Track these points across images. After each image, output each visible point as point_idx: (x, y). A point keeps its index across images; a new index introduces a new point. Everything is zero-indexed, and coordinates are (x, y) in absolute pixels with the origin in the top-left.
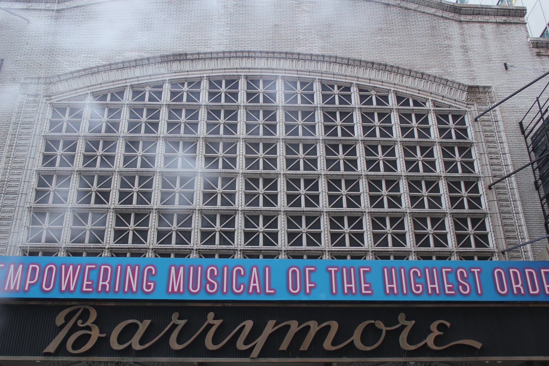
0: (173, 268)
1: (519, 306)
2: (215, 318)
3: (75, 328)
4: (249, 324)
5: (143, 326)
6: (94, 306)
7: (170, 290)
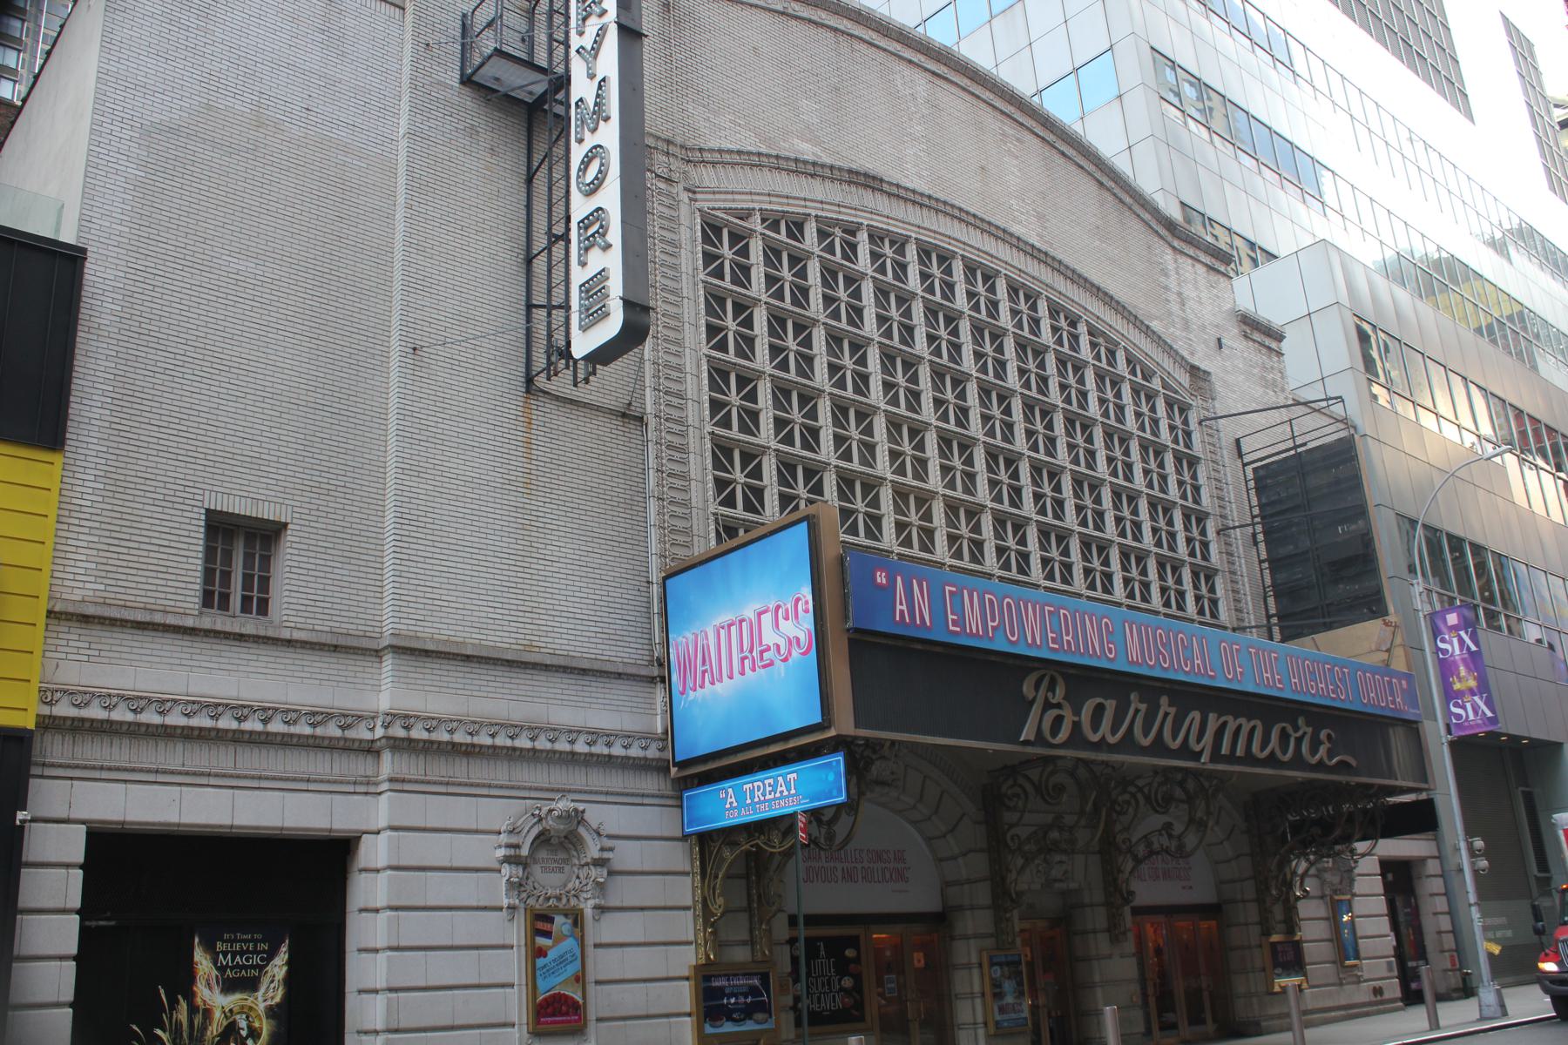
6: (1063, 675)
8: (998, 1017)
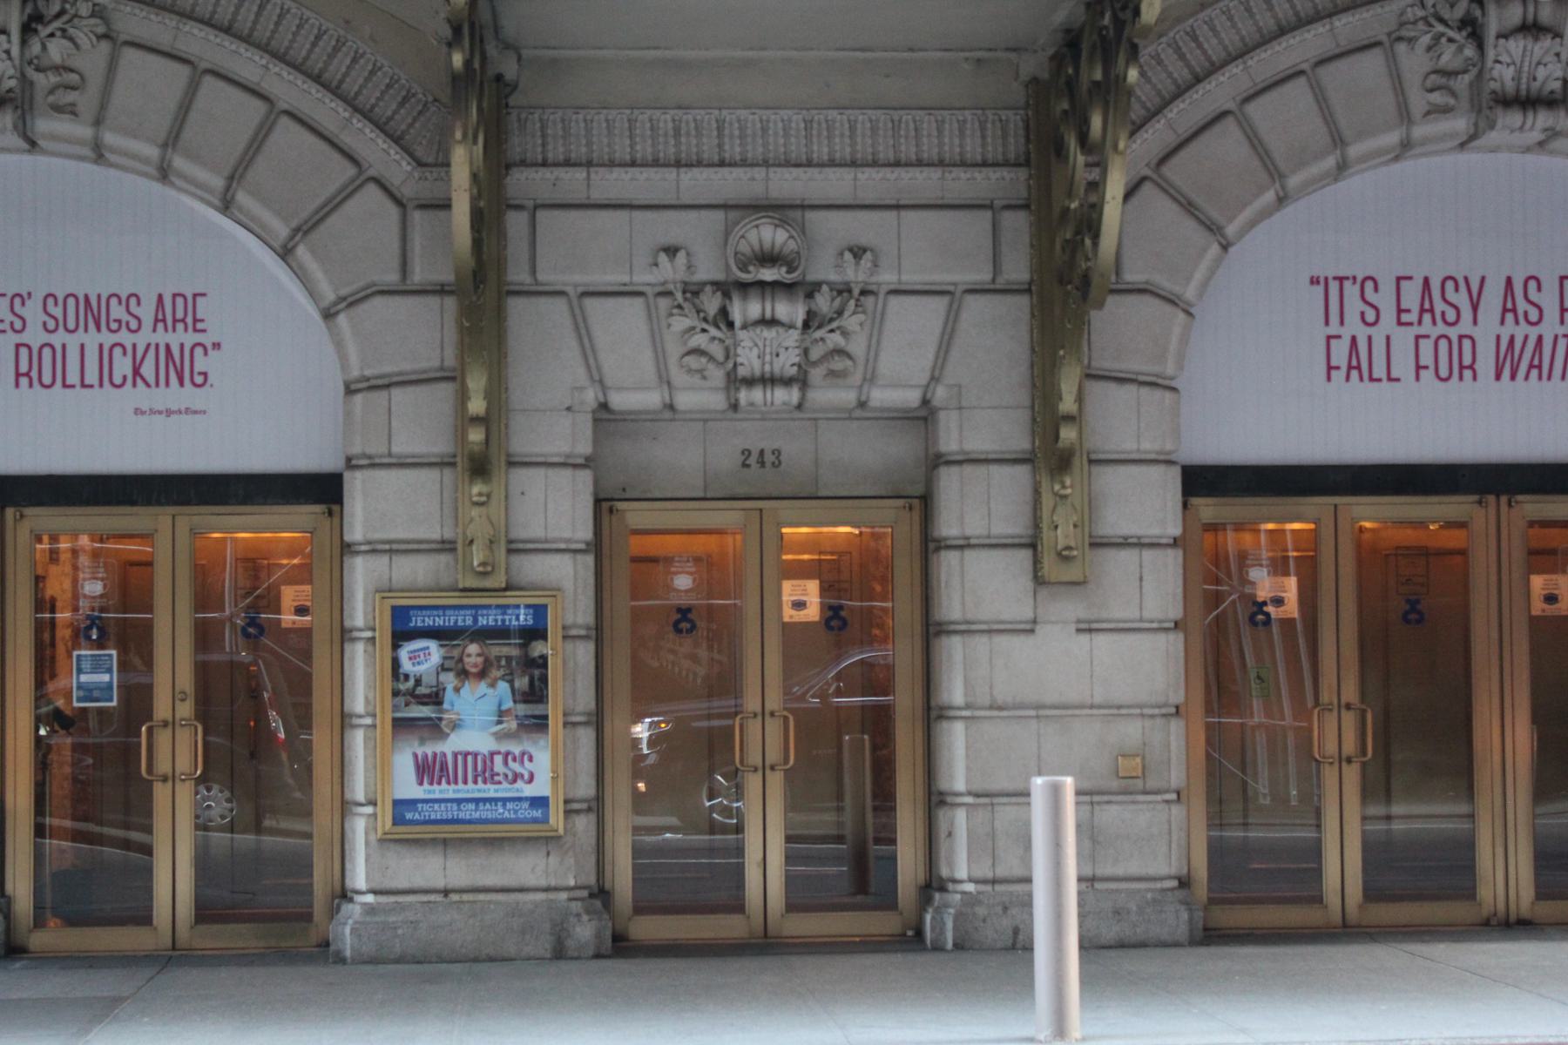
8: (407, 786)
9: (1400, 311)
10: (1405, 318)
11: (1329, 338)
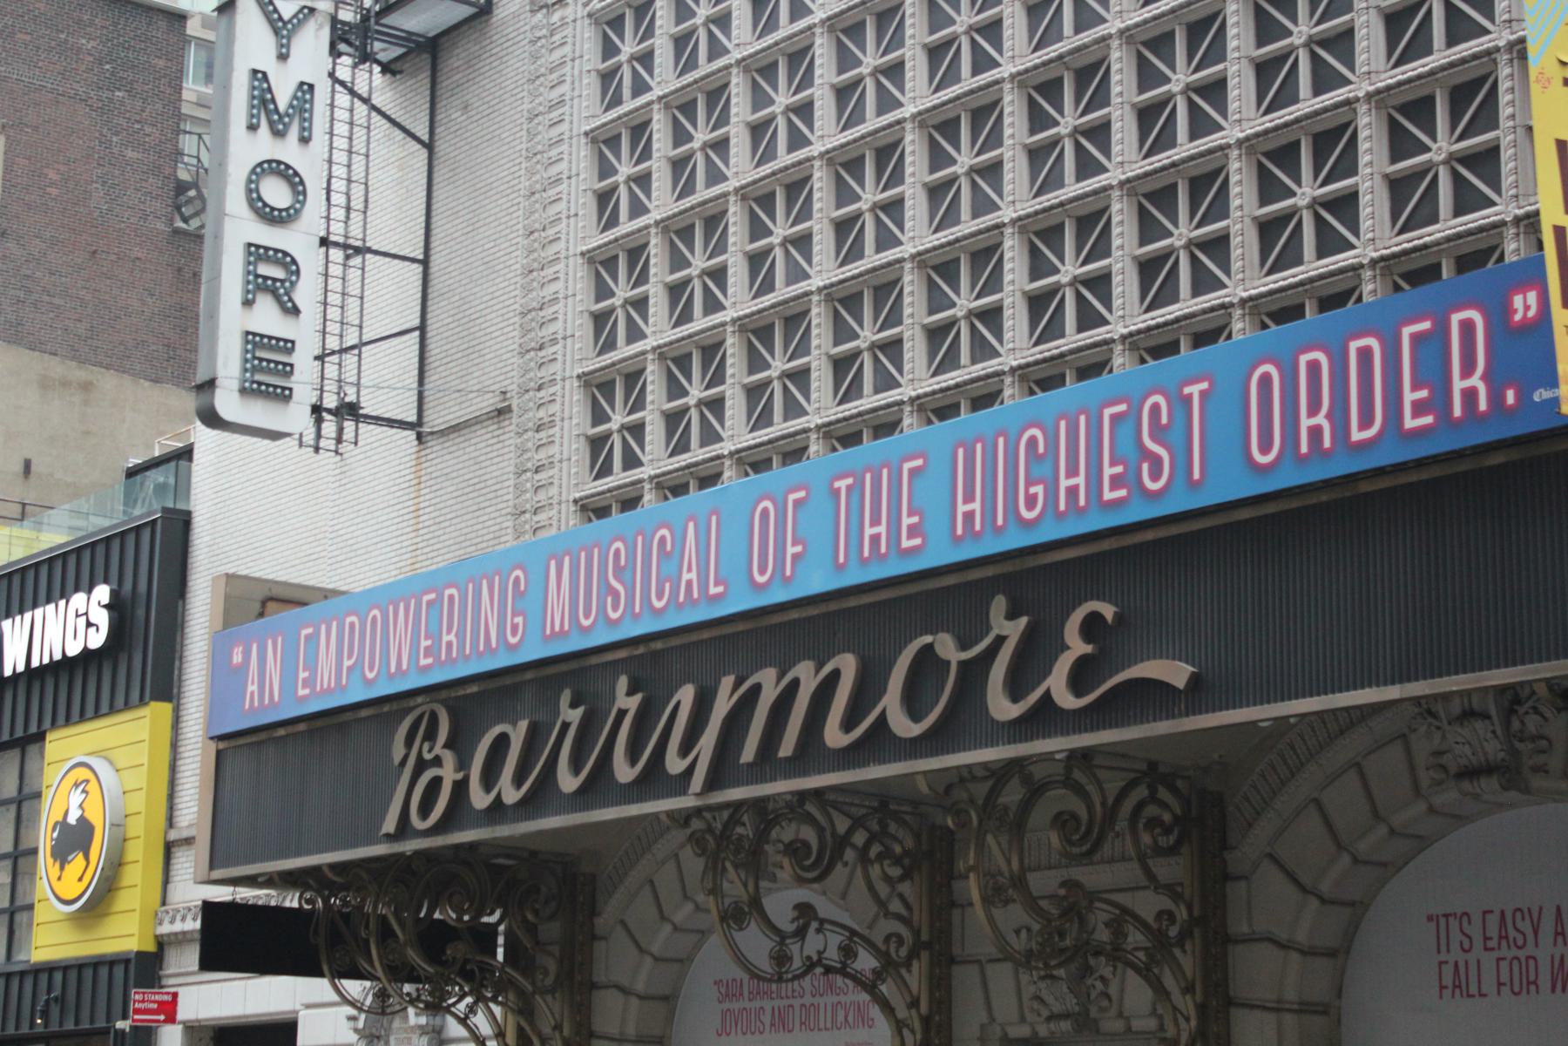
0: (553, 563)
1: (1324, 498)
2: (631, 692)
3: (421, 766)
4: (686, 695)
5: (518, 734)
6: (444, 702)
7: (548, 632)
9: (1486, 939)
10: (1492, 944)
11: (1441, 963)
